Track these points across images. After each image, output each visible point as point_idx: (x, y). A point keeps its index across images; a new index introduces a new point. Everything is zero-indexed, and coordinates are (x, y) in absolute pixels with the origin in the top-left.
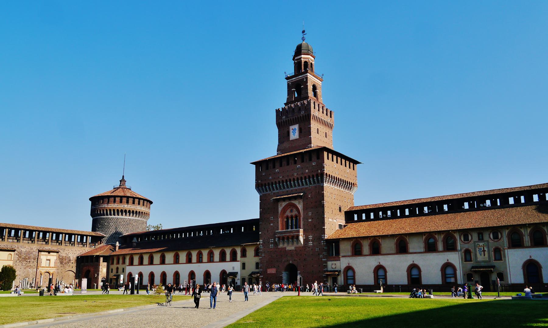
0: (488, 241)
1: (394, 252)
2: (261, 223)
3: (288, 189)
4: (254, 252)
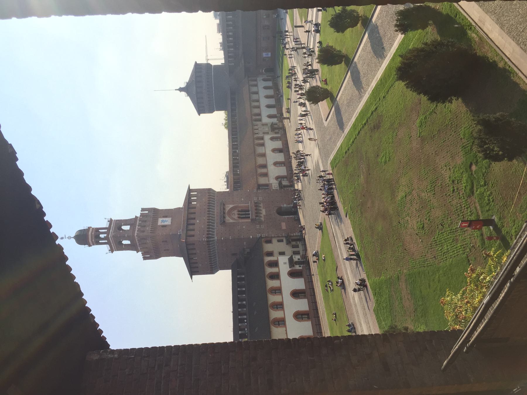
0: (259, 127)
1: (265, 158)
2: (242, 236)
3: (215, 216)
4: (268, 244)
